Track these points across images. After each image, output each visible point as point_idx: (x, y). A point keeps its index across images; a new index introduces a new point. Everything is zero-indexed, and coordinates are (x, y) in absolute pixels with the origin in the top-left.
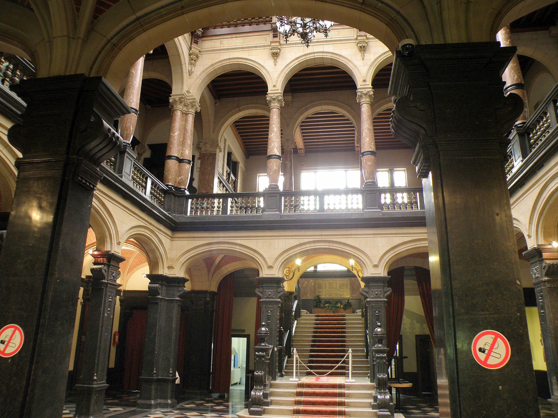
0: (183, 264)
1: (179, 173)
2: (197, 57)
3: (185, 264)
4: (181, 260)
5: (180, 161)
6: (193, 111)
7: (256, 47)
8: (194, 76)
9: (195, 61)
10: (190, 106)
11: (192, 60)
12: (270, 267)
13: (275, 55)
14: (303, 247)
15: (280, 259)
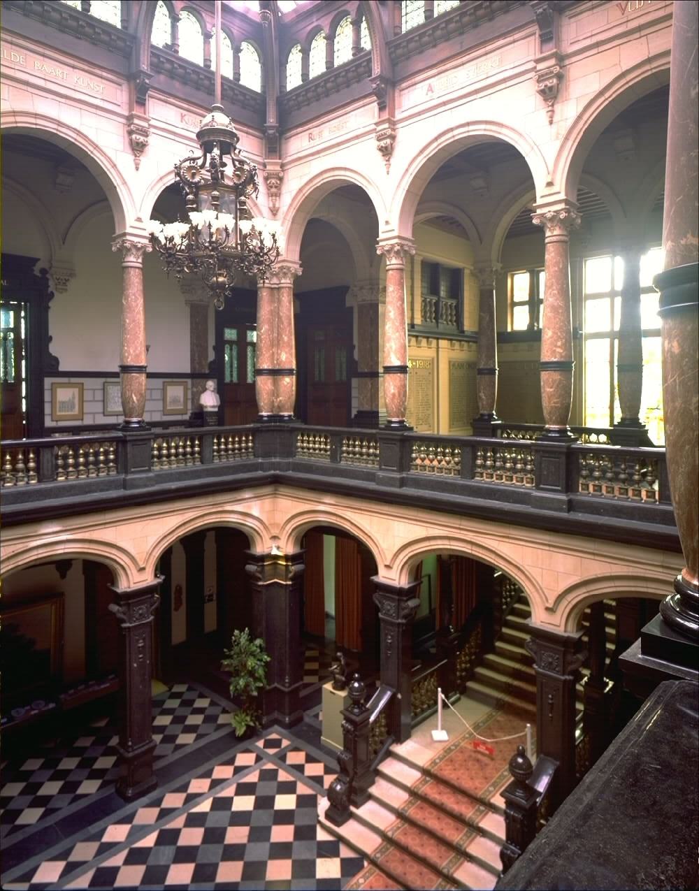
0: (291, 534)
1: (275, 393)
2: (281, 179)
3: (293, 534)
4: (287, 528)
5: (276, 373)
6: (287, 282)
7: (357, 137)
8: (281, 214)
9: (276, 187)
10: (281, 275)
11: (271, 187)
12: (388, 567)
13: (387, 152)
14: (433, 543)
15: (401, 556)
